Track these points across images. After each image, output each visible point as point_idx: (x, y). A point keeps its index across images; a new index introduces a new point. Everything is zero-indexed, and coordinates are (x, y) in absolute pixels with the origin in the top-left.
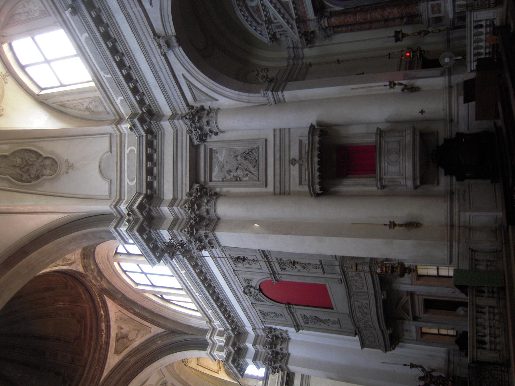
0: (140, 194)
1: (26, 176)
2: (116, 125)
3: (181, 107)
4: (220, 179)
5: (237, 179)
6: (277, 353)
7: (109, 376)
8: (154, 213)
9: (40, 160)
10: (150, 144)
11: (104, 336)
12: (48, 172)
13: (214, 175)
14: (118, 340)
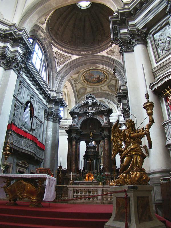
13: (156, 34)
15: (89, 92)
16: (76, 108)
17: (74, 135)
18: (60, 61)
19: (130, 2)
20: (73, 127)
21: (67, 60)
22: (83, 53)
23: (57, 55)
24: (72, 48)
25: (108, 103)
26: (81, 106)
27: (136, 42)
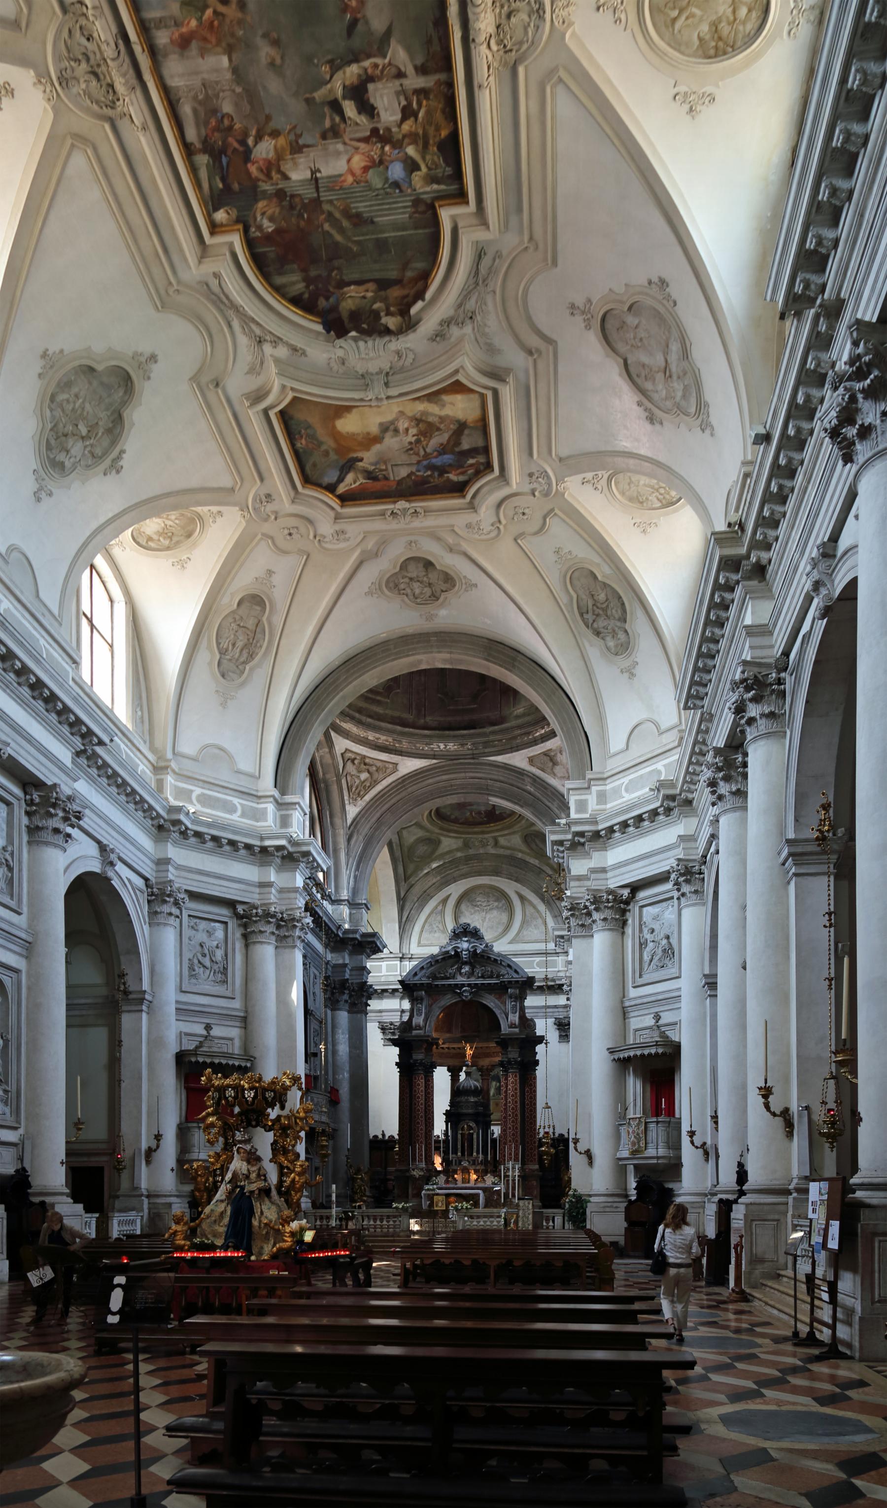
7: (498, 767)
11: (543, 731)
18: (357, 782)
22: (442, 746)
23: (349, 763)
24: (399, 728)
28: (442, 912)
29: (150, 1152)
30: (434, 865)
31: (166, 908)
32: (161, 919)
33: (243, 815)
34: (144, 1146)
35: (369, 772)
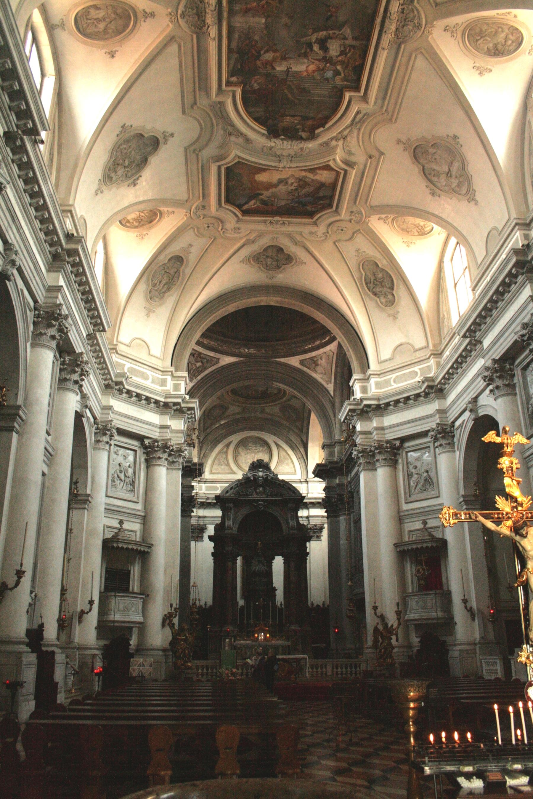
0: (378, 400)
1: (371, 286)
2: (431, 354)
3: (451, 417)
4: (409, 460)
5: (410, 476)
6: (337, 506)
8: (370, 414)
9: (389, 290)
10: (418, 396)
12: (383, 300)
13: (412, 453)
14: (311, 359)
15: (234, 414)
16: (232, 488)
17: (229, 548)
19: (379, 373)
20: (226, 531)
21: (209, 365)
22: (246, 350)
25: (278, 445)
26: (241, 484)
27: (382, 463)
28: (226, 453)
29: (82, 613)
30: (222, 422)
31: (106, 439)
32: (101, 445)
33: (153, 382)
34: (79, 609)
35: (202, 362)
